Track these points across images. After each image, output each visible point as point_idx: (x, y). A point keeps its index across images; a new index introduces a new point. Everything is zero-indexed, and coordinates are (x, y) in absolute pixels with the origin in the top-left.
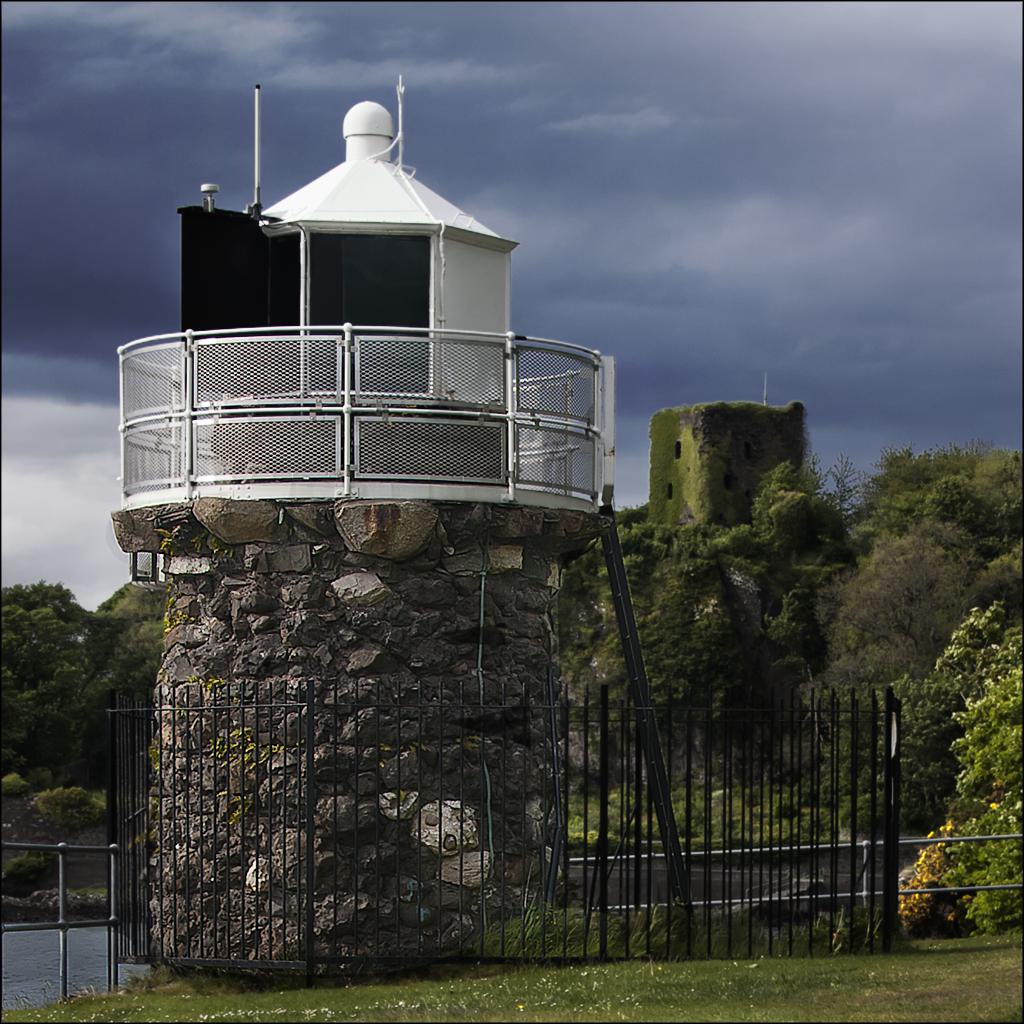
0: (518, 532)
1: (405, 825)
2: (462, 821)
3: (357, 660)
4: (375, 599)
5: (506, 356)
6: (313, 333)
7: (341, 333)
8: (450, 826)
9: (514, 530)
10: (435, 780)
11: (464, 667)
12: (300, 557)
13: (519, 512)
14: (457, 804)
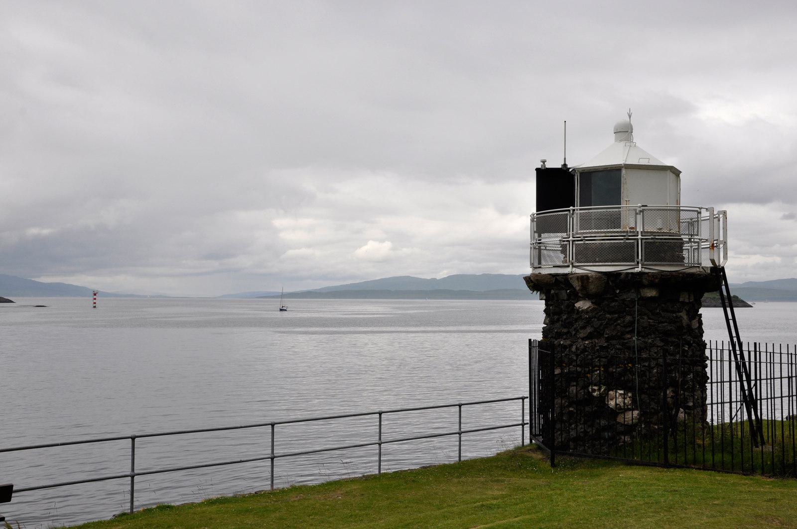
0: (647, 283)
1: (603, 398)
2: (624, 398)
3: (582, 334)
4: (591, 310)
5: (637, 214)
6: (580, 210)
7: (569, 211)
8: (620, 400)
9: (645, 282)
10: (613, 383)
11: (629, 336)
12: (564, 295)
13: (646, 275)
14: (622, 392)
